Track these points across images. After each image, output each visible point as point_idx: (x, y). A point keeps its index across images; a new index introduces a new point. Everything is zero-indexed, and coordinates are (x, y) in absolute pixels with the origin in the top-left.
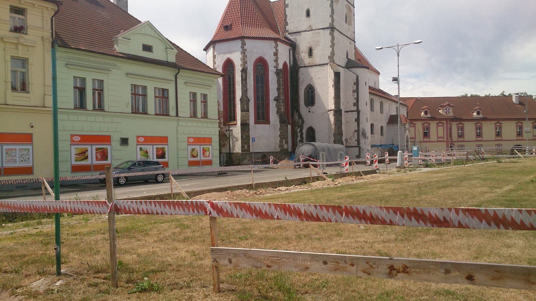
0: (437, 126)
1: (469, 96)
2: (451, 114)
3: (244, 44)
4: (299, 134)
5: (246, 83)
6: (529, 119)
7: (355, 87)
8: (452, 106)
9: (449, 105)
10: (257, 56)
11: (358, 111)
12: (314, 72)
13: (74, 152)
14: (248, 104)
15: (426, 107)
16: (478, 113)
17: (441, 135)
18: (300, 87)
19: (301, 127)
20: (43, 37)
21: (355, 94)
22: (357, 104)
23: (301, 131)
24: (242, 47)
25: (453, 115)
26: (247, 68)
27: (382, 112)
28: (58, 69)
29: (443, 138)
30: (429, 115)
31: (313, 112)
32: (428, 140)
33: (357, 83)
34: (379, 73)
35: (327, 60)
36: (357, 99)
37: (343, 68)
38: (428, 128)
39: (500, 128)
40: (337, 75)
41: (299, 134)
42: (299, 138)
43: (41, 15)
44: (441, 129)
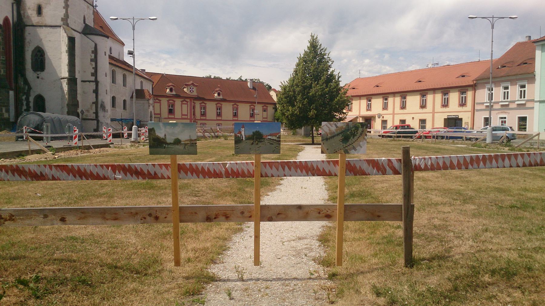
0: (182, 104)
1: (212, 77)
2: (195, 93)
4: (25, 103)
6: (259, 103)
7: (93, 55)
8: (196, 86)
9: (193, 84)
11: (97, 82)
12: (43, 33)
15: (171, 84)
16: (219, 94)
17: (185, 112)
18: (26, 48)
19: (28, 95)
21: (94, 63)
22: (95, 74)
23: (27, 99)
25: (196, 94)
27: (124, 85)
29: (187, 115)
30: (174, 93)
31: (42, 79)
32: (173, 116)
33: (95, 52)
34: (123, 44)
35: (59, 22)
36: (96, 69)
37: (80, 33)
38: (173, 106)
39: (237, 109)
40: (72, 41)
41: (25, 103)
42: (25, 107)
44: (185, 107)
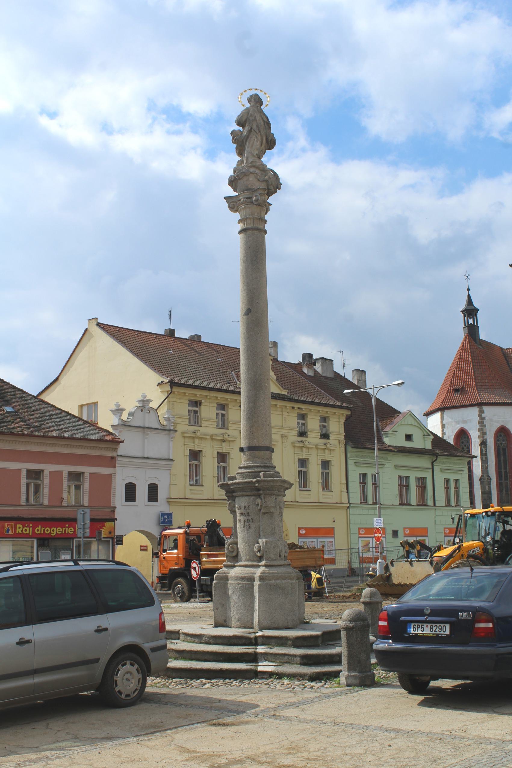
3: (481, 412)
5: (486, 458)
10: (498, 425)
13: (361, 545)
14: (489, 484)
20: (339, 440)
24: (480, 415)
26: (486, 440)
28: (350, 467)
43: (337, 420)
